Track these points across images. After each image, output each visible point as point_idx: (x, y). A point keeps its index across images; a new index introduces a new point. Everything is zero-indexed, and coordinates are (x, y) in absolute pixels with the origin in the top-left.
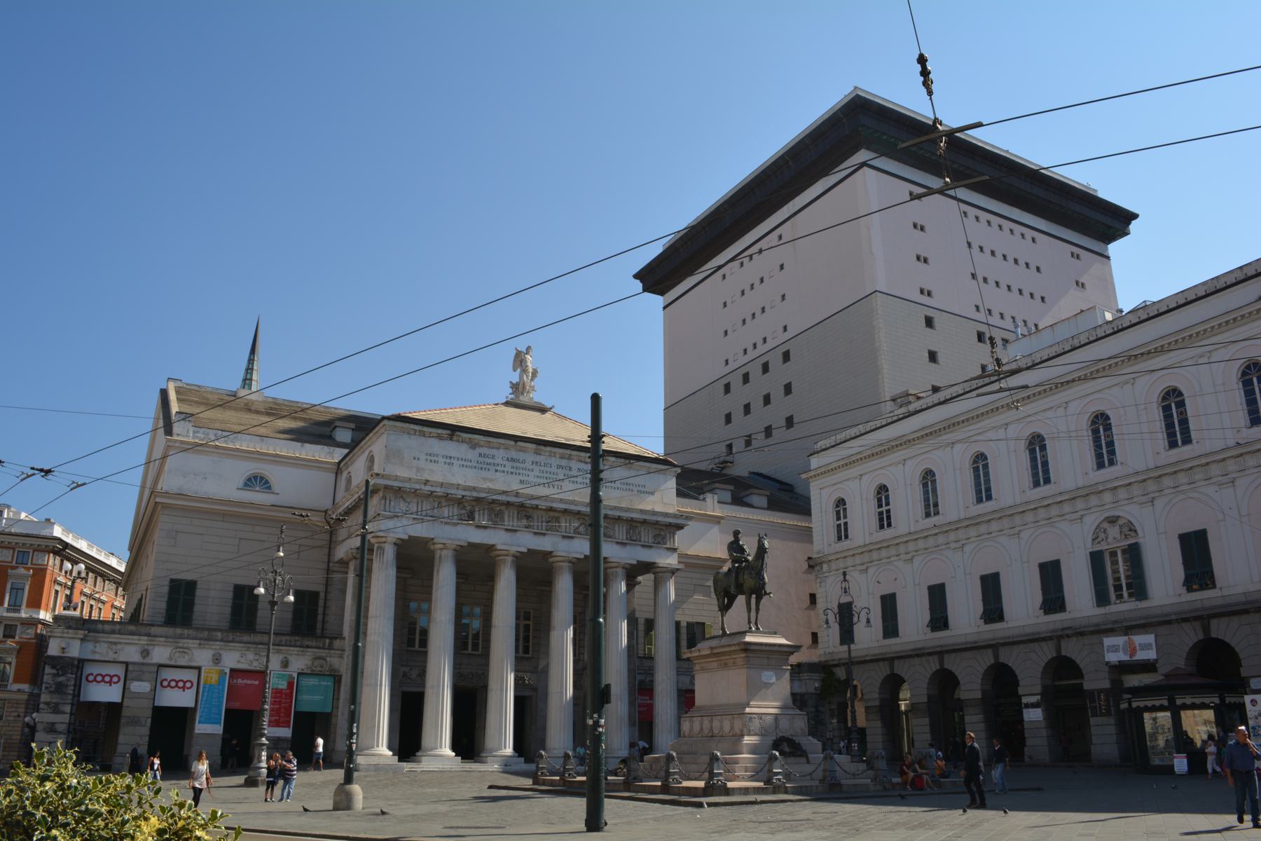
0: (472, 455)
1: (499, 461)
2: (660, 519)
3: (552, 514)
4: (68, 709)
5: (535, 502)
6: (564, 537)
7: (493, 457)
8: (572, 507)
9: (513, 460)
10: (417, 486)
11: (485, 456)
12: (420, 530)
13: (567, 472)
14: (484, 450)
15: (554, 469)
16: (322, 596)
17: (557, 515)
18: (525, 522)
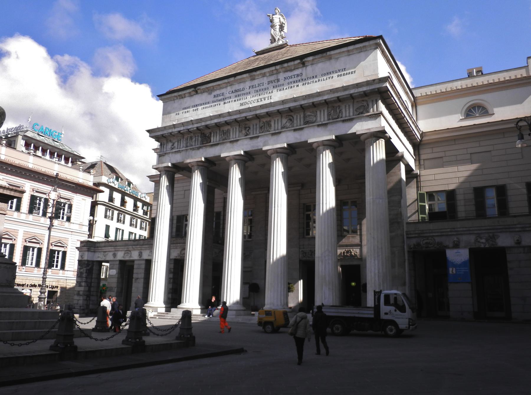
0: (210, 98)
1: (228, 95)
2: (352, 91)
3: (264, 120)
4: (83, 284)
5: (244, 115)
6: (273, 134)
7: (223, 94)
8: (271, 109)
9: (236, 91)
10: (170, 131)
11: (218, 95)
12: (177, 158)
13: (276, 84)
14: (218, 92)
15: (266, 86)
16: (222, 214)
17: (268, 119)
18: (244, 132)
